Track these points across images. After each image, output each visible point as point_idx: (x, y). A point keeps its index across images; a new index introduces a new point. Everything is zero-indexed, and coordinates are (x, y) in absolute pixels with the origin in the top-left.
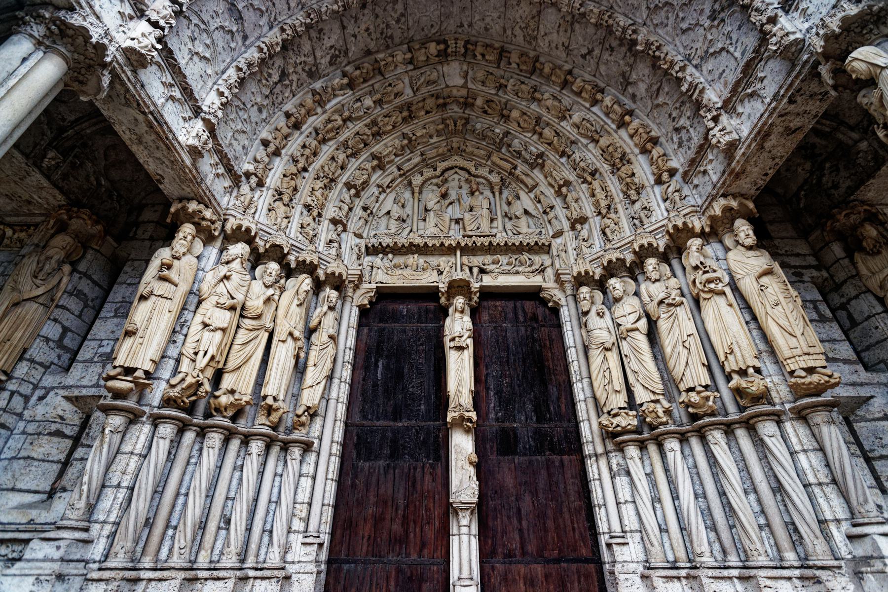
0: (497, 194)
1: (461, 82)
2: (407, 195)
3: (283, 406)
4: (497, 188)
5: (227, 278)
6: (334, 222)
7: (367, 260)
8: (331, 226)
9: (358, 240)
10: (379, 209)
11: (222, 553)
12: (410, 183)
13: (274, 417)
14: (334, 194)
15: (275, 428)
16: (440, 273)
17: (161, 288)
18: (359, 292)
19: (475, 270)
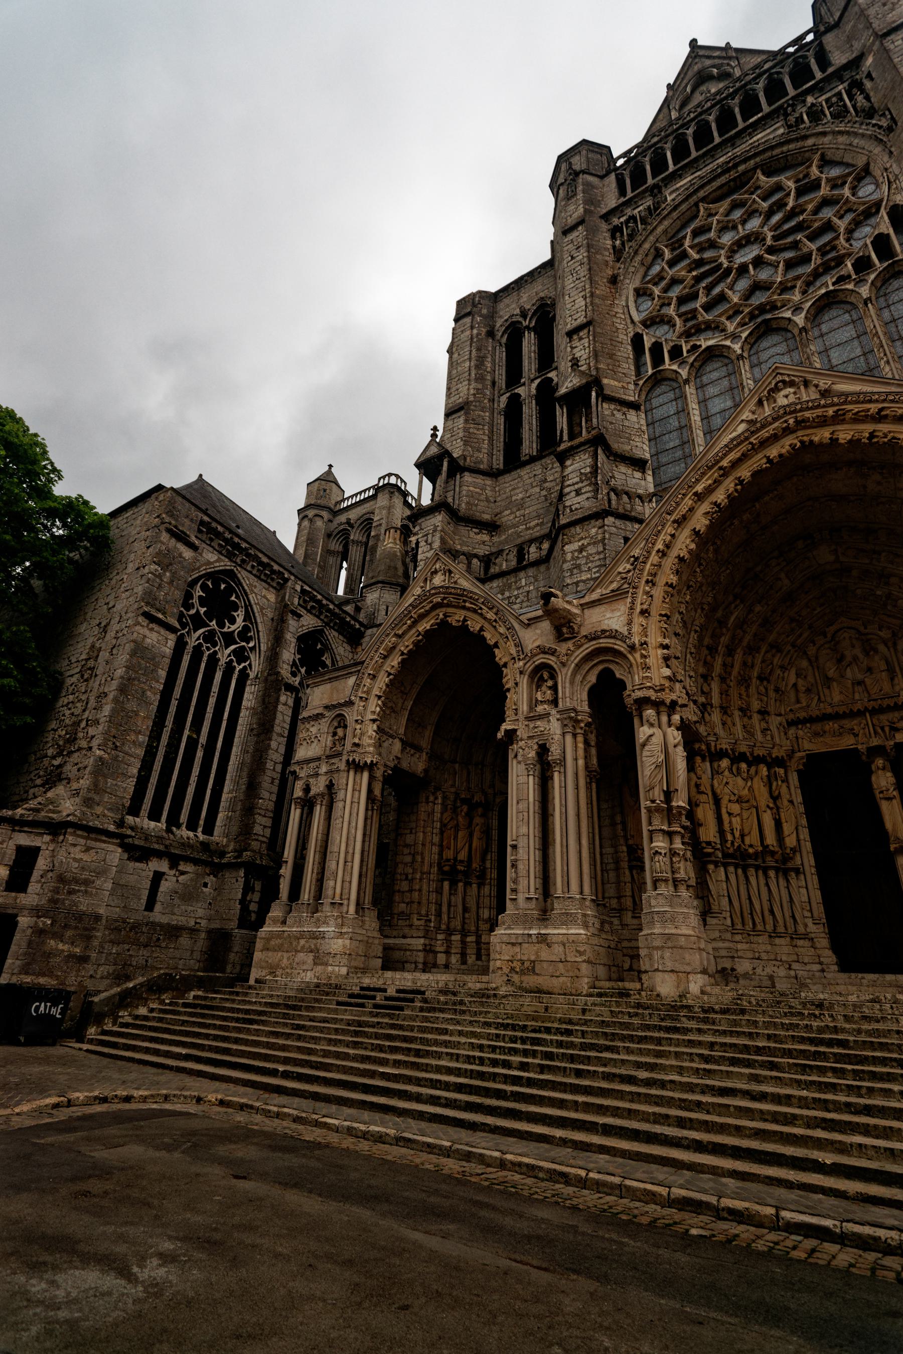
0: (892, 650)
1: (832, 558)
2: (805, 663)
3: (777, 849)
4: (890, 644)
5: (727, 783)
6: (759, 712)
7: (792, 731)
8: (759, 717)
9: (779, 718)
10: (786, 685)
11: (775, 926)
12: (805, 653)
13: (777, 857)
14: (752, 690)
15: (776, 862)
16: (856, 735)
17: (703, 798)
18: (793, 761)
19: (887, 729)
